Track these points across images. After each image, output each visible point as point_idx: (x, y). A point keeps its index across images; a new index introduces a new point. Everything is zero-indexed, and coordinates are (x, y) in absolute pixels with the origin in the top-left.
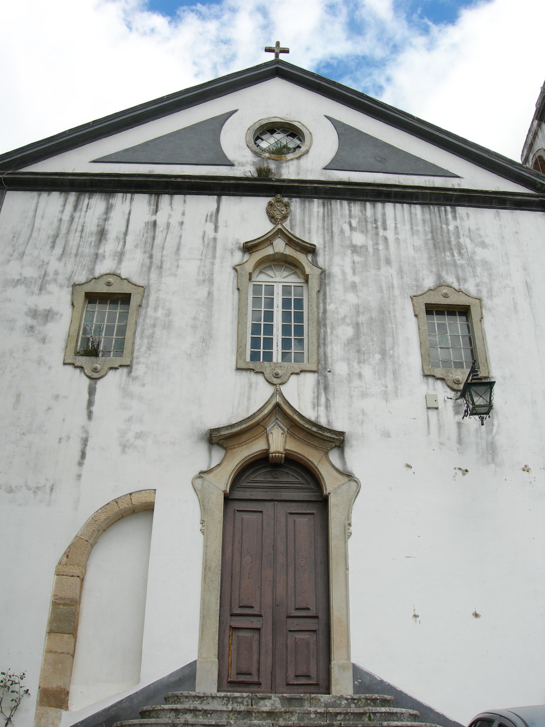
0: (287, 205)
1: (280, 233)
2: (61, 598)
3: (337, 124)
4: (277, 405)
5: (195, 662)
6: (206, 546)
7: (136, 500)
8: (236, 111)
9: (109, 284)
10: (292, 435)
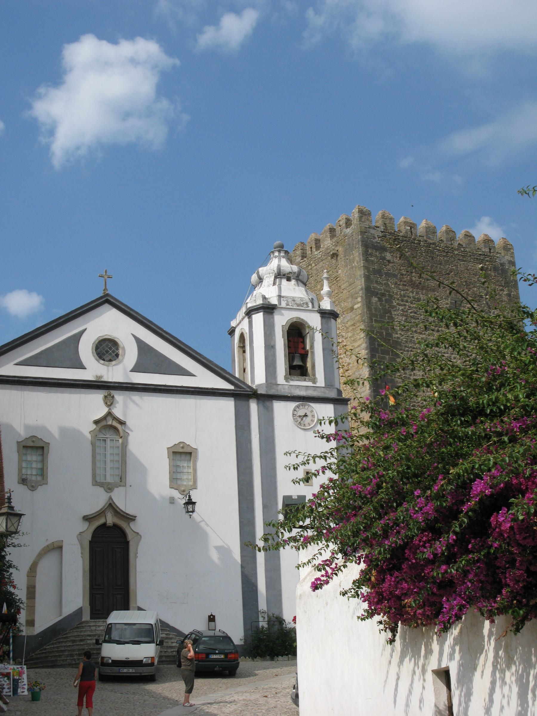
5: (82, 607)
6: (83, 563)
7: (55, 545)
9: (33, 442)
10: (115, 515)
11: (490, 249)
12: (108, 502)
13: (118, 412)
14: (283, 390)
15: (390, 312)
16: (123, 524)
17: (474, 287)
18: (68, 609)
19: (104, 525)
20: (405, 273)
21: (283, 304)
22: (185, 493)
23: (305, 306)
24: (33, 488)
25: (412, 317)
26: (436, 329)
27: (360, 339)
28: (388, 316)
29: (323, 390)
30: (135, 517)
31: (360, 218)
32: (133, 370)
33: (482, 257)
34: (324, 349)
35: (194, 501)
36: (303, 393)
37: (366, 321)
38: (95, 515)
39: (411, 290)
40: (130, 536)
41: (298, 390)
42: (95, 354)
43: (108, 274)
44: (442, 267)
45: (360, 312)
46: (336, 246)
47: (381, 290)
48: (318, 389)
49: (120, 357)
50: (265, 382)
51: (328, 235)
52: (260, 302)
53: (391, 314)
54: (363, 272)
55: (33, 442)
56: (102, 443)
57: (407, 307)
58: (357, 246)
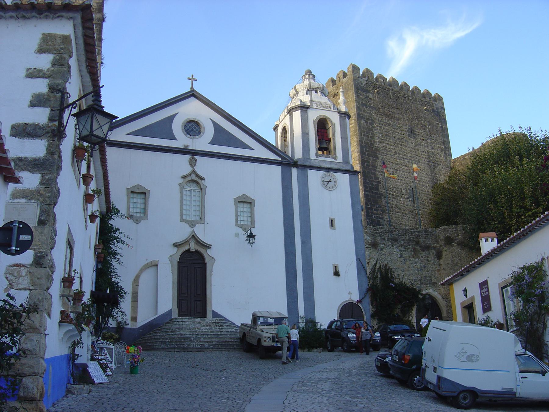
0: (196, 160)
1: (194, 172)
2: (134, 292)
3: (215, 124)
4: (193, 235)
5: (172, 309)
6: (173, 277)
8: (178, 113)
9: (138, 189)
10: (197, 244)
11: (430, 99)
12: (191, 233)
13: (199, 170)
14: (314, 163)
15: (372, 130)
16: (202, 250)
17: (422, 120)
18: (162, 310)
19: (188, 251)
20: (381, 107)
21: (314, 106)
22: (247, 230)
23: (329, 108)
24: (137, 221)
25: (386, 135)
26: (400, 143)
27: (353, 146)
28: (371, 133)
29: (342, 164)
30: (211, 245)
31: (353, 71)
32: (210, 143)
33: (426, 103)
34: (341, 138)
35: (254, 234)
36: (328, 166)
37: (358, 134)
38: (182, 243)
39: (385, 118)
40: (207, 260)
41: (325, 163)
42: (184, 131)
43: (194, 78)
44: (403, 106)
45: (354, 129)
46: (336, 90)
47: (367, 116)
48: (338, 163)
49: (201, 134)
50: (302, 157)
51: (331, 84)
52: (298, 103)
53: (373, 132)
54: (355, 104)
55: (138, 189)
56: (188, 193)
57: (383, 128)
58: (351, 88)
